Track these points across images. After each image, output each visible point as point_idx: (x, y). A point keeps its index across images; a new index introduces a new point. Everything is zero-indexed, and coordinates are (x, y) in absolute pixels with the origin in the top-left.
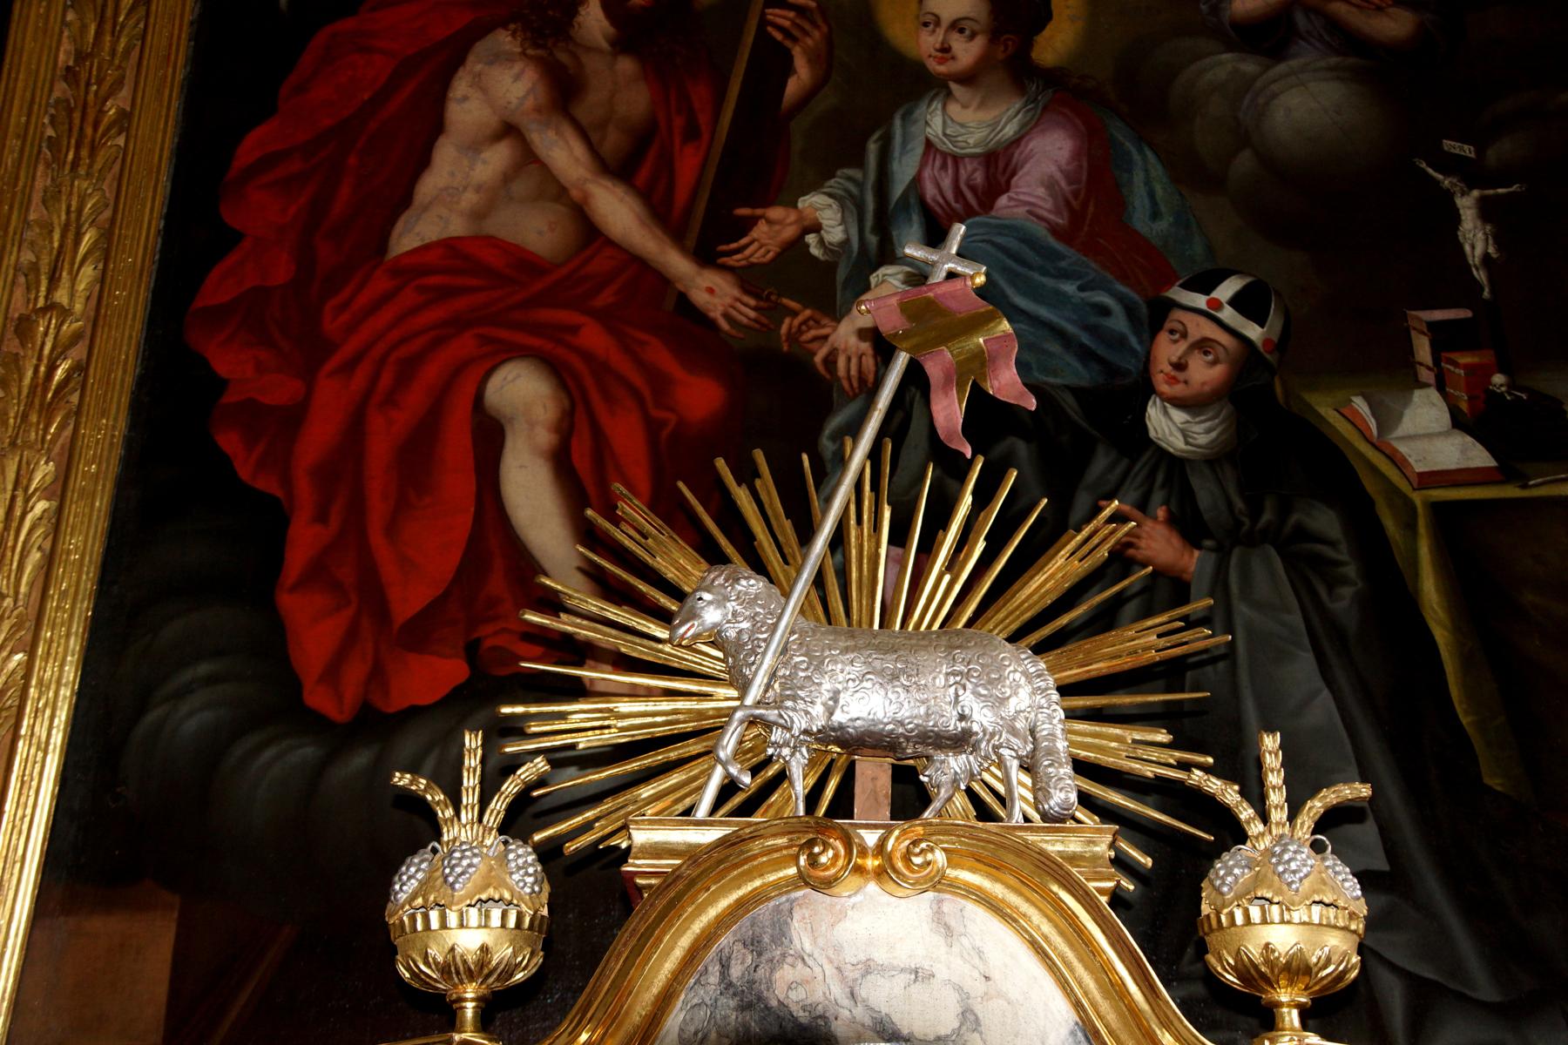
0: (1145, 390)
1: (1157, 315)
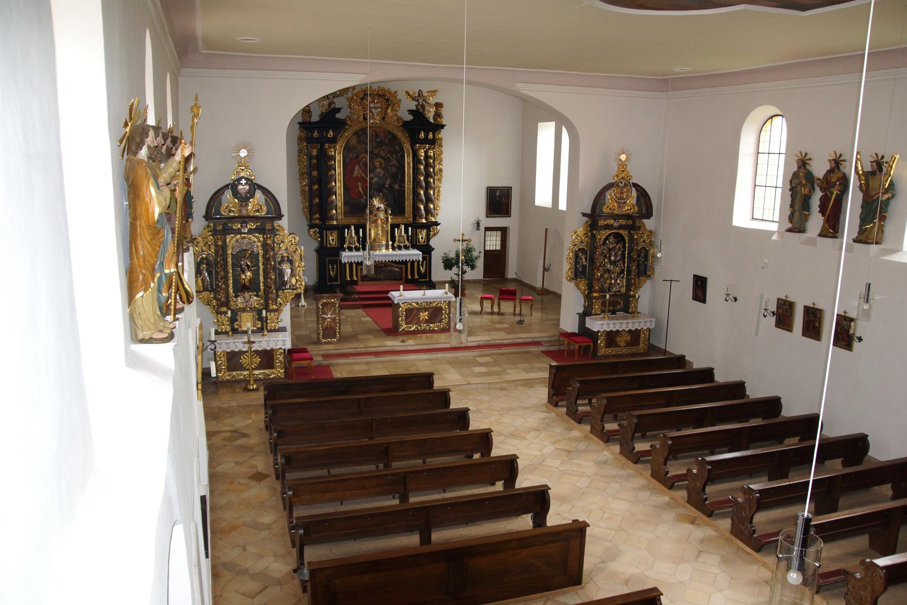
0: (385, 184)
1: (386, 181)
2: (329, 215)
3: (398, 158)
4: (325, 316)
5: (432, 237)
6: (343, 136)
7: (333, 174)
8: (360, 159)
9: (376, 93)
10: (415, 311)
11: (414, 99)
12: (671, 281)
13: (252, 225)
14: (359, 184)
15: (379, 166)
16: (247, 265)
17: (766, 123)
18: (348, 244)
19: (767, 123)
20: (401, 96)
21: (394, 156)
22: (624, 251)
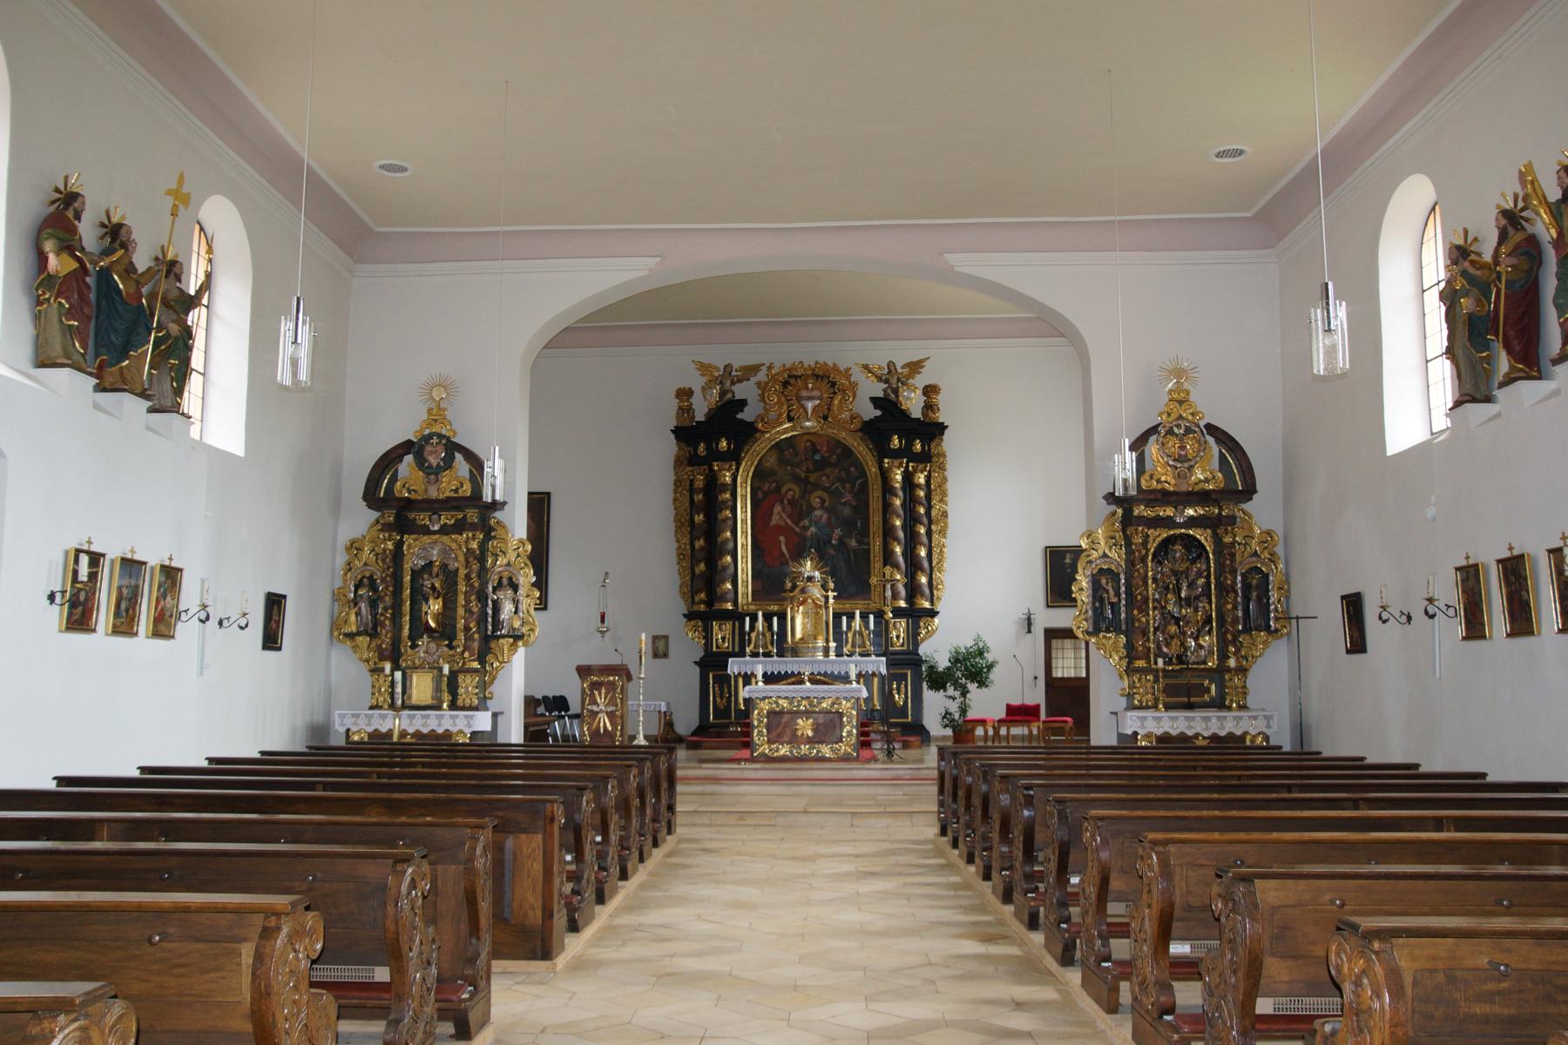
1: (833, 532)
2: (719, 591)
3: (856, 490)
4: (595, 708)
5: (923, 640)
6: (751, 452)
7: (728, 518)
8: (784, 490)
9: (810, 372)
10: (786, 718)
11: (880, 379)
12: (1297, 618)
13: (447, 519)
14: (782, 539)
15: (819, 505)
16: (433, 588)
17: (1426, 224)
18: (755, 647)
19: (1429, 223)
20: (858, 376)
21: (848, 485)
22: (1208, 577)
